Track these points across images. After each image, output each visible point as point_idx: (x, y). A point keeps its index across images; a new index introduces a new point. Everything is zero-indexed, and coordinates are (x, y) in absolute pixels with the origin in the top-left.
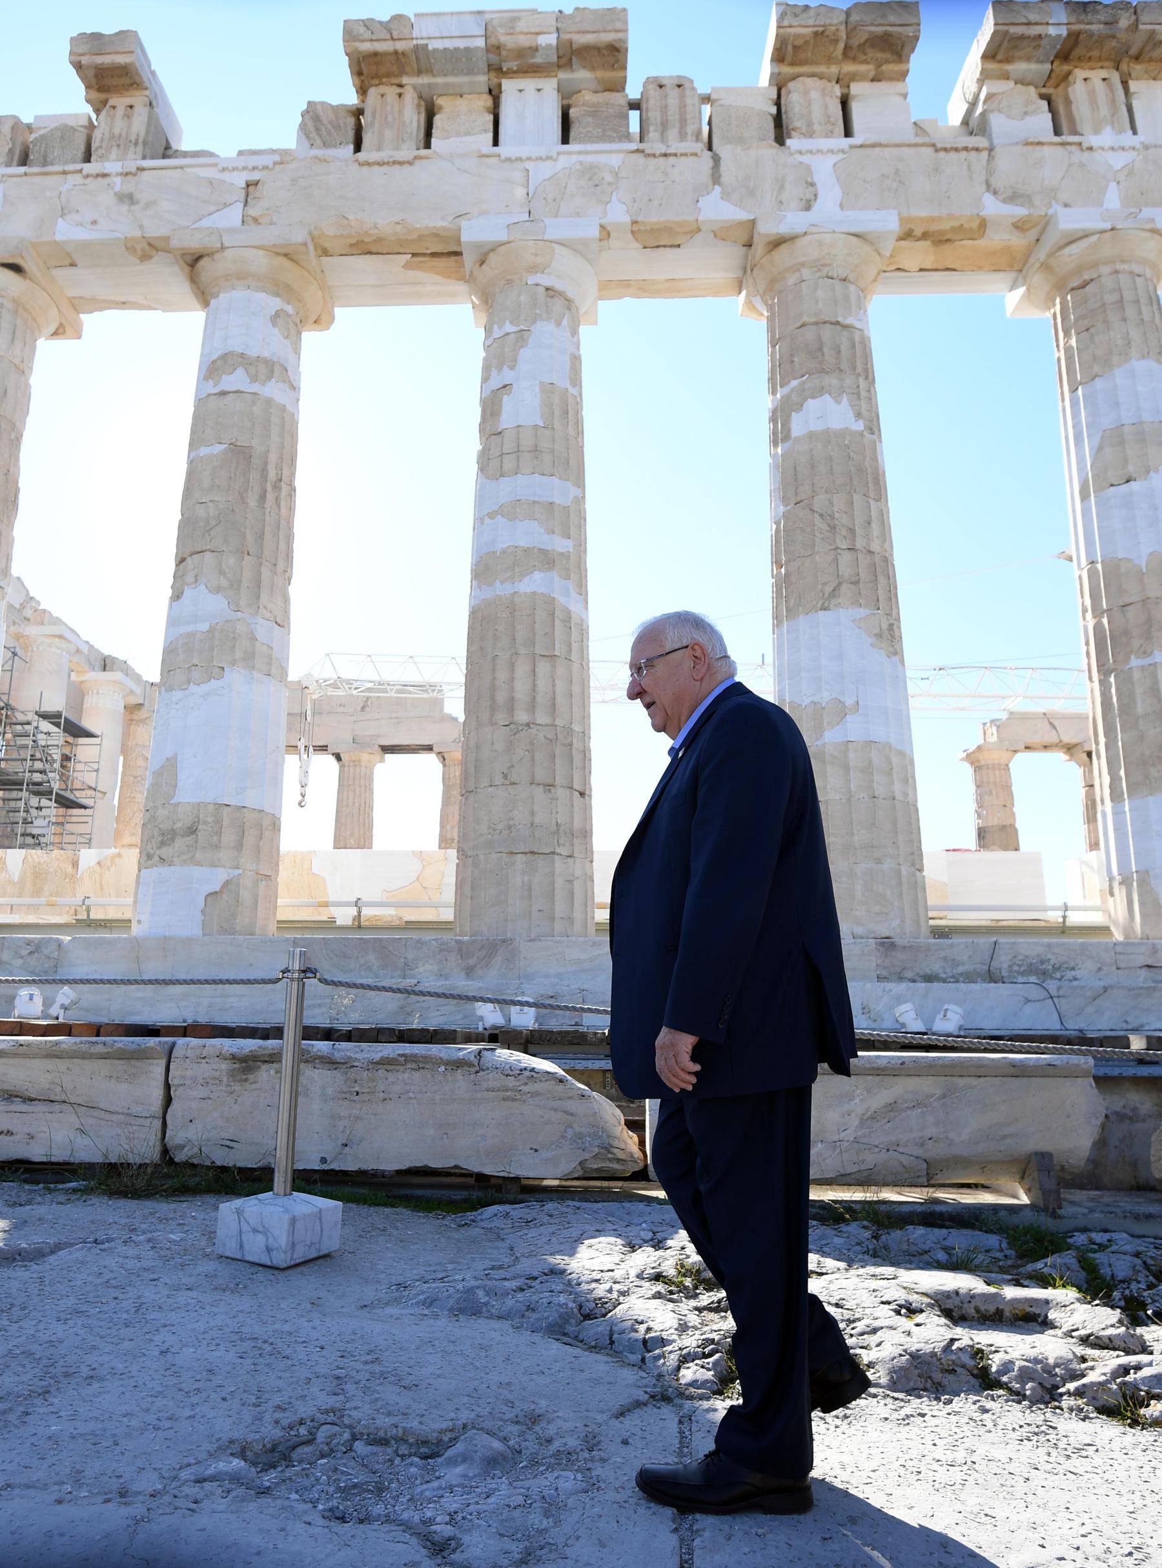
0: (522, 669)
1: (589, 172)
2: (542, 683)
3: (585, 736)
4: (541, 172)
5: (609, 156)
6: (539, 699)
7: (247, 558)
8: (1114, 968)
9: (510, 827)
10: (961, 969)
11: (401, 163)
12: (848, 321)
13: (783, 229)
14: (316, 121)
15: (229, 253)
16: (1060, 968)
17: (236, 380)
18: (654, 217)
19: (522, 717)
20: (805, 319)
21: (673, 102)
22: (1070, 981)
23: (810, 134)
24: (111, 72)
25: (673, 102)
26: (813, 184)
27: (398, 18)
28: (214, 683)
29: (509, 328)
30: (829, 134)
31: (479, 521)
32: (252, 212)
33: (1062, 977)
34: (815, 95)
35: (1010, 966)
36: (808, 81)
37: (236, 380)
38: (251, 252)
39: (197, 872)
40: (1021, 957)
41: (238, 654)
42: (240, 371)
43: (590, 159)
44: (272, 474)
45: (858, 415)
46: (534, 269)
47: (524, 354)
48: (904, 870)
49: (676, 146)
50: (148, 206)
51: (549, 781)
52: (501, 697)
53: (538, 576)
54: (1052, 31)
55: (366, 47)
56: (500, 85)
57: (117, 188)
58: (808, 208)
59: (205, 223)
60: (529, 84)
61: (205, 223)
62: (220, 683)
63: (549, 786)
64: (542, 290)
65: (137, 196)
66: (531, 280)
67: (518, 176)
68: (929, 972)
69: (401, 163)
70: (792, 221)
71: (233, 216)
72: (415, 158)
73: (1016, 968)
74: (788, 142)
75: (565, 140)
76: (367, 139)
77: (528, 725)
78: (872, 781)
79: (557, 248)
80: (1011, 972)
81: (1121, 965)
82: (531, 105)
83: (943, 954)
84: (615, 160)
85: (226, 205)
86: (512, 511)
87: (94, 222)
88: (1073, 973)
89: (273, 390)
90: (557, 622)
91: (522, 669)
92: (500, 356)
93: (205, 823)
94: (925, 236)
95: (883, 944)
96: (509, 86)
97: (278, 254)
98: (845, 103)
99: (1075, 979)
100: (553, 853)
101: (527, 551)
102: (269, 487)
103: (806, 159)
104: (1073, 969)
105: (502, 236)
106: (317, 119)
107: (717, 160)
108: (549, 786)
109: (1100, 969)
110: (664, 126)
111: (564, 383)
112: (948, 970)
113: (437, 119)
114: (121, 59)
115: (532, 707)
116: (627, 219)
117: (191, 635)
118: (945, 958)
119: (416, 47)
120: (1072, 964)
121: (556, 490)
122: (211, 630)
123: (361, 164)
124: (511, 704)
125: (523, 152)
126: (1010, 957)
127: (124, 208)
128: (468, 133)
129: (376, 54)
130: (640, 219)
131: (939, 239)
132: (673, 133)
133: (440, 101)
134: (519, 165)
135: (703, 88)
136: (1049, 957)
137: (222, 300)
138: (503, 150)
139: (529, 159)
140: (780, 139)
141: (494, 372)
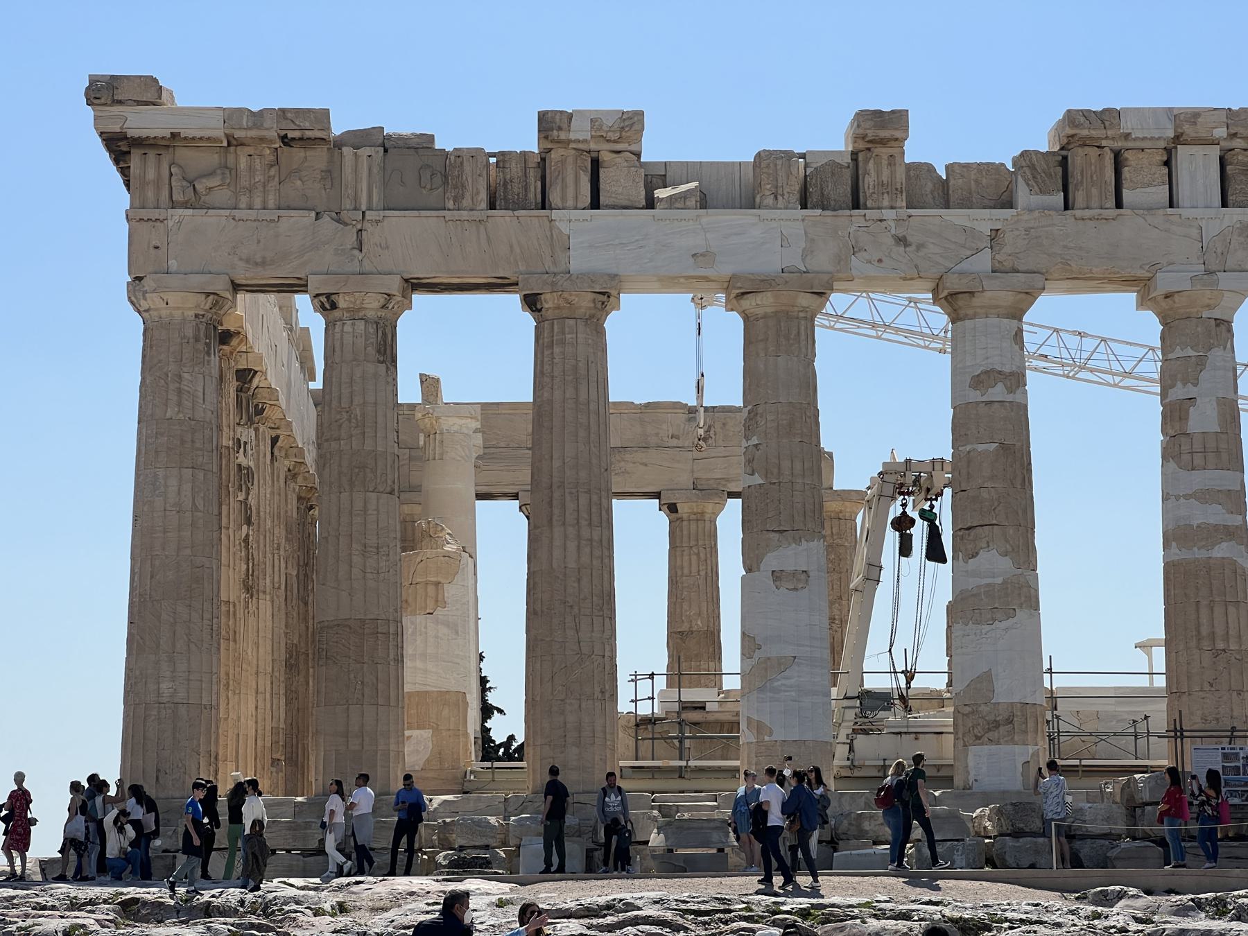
0: (1219, 611)
9: (1217, 719)
29: (1191, 353)
39: (1004, 749)
47: (1204, 375)
50: (920, 246)
52: (1205, 631)
53: (1224, 545)
59: (964, 266)
60: (1198, 150)
62: (1014, 620)
64: (1213, 322)
65: (909, 238)
67: (1195, 232)
75: (1224, 204)
76: (1079, 197)
82: (1198, 170)
87: (880, 261)
91: (1219, 611)
101: (1216, 527)
106: (1032, 167)
111: (1231, 395)
115: (1226, 638)
122: (1005, 582)
124: (1212, 636)
128: (1150, 185)
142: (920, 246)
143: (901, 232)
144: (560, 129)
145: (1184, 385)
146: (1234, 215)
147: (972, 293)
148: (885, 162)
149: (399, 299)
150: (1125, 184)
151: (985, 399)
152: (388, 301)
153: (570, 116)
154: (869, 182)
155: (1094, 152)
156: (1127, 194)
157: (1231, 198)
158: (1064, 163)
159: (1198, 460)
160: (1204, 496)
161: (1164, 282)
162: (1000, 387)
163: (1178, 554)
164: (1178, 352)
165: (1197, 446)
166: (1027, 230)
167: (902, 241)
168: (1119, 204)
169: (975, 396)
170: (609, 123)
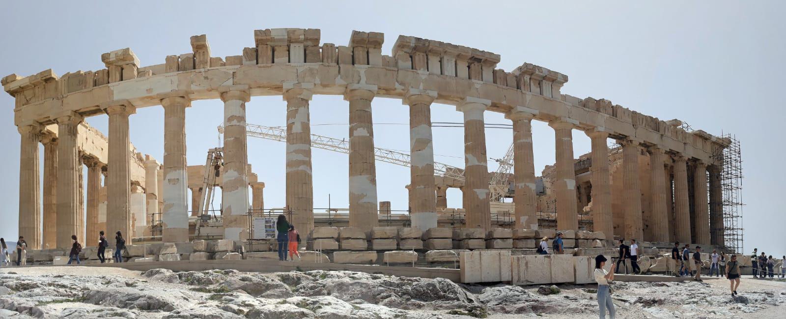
1: (311, 70)
3: (312, 199)
4: (300, 70)
5: (316, 66)
12: (367, 110)
13: (353, 88)
14: (246, 50)
17: (235, 122)
20: (358, 109)
21: (330, 51)
23: (359, 63)
24: (199, 43)
25: (330, 51)
26: (360, 76)
27: (267, 30)
30: (364, 64)
31: (287, 153)
32: (235, 80)
34: (361, 52)
36: (360, 48)
37: (235, 122)
38: (236, 91)
42: (235, 121)
43: (311, 67)
45: (368, 133)
49: (331, 64)
50: (211, 79)
54: (411, 45)
55: (260, 38)
56: (290, 45)
58: (359, 83)
59: (225, 84)
60: (297, 45)
61: (225, 84)
63: (306, 210)
66: (299, 97)
67: (295, 71)
70: (355, 86)
71: (230, 82)
74: (355, 65)
76: (260, 60)
82: (297, 52)
84: (317, 67)
85: (229, 79)
86: (297, 152)
87: (200, 85)
89: (241, 124)
92: (291, 115)
94: (384, 89)
96: (292, 45)
98: (368, 53)
103: (359, 70)
105: (292, 87)
106: (247, 53)
107: (339, 67)
110: (328, 58)
113: (275, 53)
116: (320, 83)
117: (231, 180)
119: (271, 38)
121: (303, 147)
123: (259, 67)
125: (296, 64)
127: (206, 80)
129: (262, 40)
131: (386, 90)
132: (330, 60)
133: (276, 48)
135: (336, 45)
137: (229, 102)
138: (292, 64)
140: (353, 64)
141: (290, 119)
142: (211, 79)
143: (206, 76)
144: (107, 59)
145: (292, 118)
146: (308, 65)
147: (227, 92)
148: (201, 55)
149: (73, 117)
150: (275, 57)
151: (231, 125)
152: (70, 118)
153: (110, 54)
154: (197, 61)
155: (265, 46)
156: (275, 60)
157: (307, 61)
158: (257, 51)
159: (295, 141)
160: (297, 152)
161: (286, 86)
162: (235, 121)
163: (290, 170)
164: (291, 109)
165: (295, 137)
166: (244, 72)
167: (206, 78)
168: (273, 62)
169: (229, 124)
170: (120, 53)
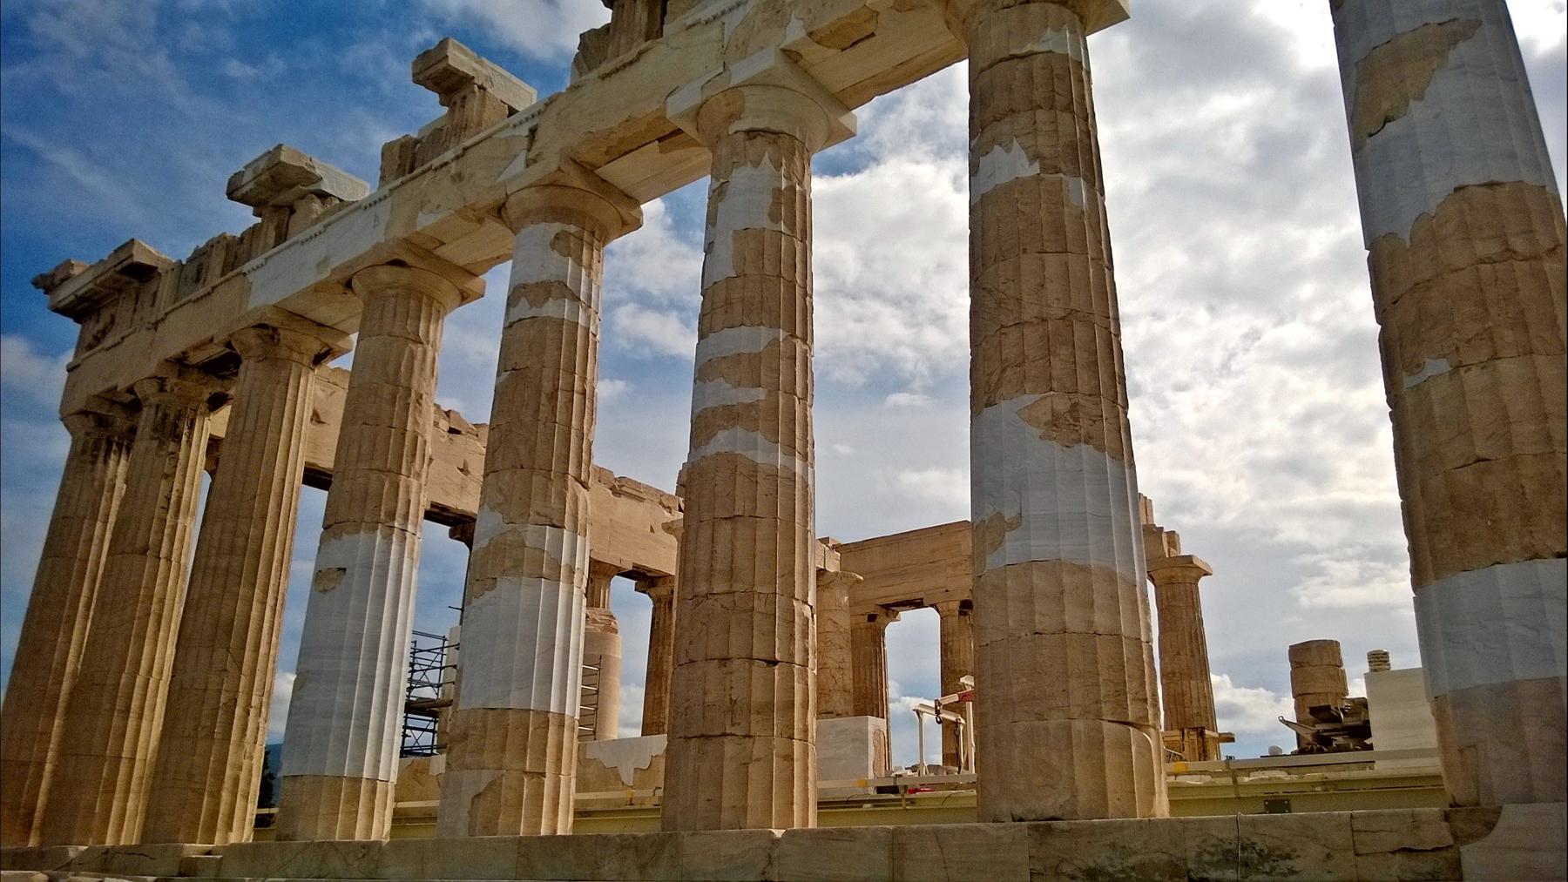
2: (722, 549)
6: (718, 566)
7: (519, 472)
8: (1351, 853)
10: (1132, 861)
11: (631, 63)
15: (512, 199)
16: (1269, 855)
18: (828, 20)
19: (703, 588)
22: (1285, 875)
28: (488, 595)
32: (531, 155)
33: (1273, 869)
35: (1199, 855)
38: (524, 193)
40: (1214, 841)
41: (508, 563)
44: (547, 386)
46: (733, 117)
48: (1079, 725)
51: (724, 654)
57: (453, 172)
62: (493, 593)
64: (742, 136)
68: (1092, 865)
69: (631, 63)
71: (519, 164)
72: (640, 54)
73: (1206, 857)
77: (706, 596)
78: (1033, 613)
79: (746, 91)
80: (1200, 862)
81: (1363, 849)
83: (1110, 839)
88: (1289, 863)
90: (739, 479)
93: (474, 728)
95: (1036, 828)
97: (547, 186)
99: (1293, 872)
100: (724, 735)
102: (543, 399)
104: (1288, 857)
108: (724, 660)
109: (1328, 856)
112: (1117, 862)
114: (441, 66)
118: (1113, 846)
120: (1288, 850)
126: (1198, 841)
130: (814, 28)
134: (718, 22)
136: (1254, 839)
139: (723, 13)
